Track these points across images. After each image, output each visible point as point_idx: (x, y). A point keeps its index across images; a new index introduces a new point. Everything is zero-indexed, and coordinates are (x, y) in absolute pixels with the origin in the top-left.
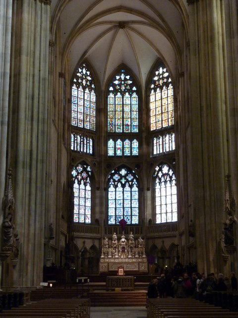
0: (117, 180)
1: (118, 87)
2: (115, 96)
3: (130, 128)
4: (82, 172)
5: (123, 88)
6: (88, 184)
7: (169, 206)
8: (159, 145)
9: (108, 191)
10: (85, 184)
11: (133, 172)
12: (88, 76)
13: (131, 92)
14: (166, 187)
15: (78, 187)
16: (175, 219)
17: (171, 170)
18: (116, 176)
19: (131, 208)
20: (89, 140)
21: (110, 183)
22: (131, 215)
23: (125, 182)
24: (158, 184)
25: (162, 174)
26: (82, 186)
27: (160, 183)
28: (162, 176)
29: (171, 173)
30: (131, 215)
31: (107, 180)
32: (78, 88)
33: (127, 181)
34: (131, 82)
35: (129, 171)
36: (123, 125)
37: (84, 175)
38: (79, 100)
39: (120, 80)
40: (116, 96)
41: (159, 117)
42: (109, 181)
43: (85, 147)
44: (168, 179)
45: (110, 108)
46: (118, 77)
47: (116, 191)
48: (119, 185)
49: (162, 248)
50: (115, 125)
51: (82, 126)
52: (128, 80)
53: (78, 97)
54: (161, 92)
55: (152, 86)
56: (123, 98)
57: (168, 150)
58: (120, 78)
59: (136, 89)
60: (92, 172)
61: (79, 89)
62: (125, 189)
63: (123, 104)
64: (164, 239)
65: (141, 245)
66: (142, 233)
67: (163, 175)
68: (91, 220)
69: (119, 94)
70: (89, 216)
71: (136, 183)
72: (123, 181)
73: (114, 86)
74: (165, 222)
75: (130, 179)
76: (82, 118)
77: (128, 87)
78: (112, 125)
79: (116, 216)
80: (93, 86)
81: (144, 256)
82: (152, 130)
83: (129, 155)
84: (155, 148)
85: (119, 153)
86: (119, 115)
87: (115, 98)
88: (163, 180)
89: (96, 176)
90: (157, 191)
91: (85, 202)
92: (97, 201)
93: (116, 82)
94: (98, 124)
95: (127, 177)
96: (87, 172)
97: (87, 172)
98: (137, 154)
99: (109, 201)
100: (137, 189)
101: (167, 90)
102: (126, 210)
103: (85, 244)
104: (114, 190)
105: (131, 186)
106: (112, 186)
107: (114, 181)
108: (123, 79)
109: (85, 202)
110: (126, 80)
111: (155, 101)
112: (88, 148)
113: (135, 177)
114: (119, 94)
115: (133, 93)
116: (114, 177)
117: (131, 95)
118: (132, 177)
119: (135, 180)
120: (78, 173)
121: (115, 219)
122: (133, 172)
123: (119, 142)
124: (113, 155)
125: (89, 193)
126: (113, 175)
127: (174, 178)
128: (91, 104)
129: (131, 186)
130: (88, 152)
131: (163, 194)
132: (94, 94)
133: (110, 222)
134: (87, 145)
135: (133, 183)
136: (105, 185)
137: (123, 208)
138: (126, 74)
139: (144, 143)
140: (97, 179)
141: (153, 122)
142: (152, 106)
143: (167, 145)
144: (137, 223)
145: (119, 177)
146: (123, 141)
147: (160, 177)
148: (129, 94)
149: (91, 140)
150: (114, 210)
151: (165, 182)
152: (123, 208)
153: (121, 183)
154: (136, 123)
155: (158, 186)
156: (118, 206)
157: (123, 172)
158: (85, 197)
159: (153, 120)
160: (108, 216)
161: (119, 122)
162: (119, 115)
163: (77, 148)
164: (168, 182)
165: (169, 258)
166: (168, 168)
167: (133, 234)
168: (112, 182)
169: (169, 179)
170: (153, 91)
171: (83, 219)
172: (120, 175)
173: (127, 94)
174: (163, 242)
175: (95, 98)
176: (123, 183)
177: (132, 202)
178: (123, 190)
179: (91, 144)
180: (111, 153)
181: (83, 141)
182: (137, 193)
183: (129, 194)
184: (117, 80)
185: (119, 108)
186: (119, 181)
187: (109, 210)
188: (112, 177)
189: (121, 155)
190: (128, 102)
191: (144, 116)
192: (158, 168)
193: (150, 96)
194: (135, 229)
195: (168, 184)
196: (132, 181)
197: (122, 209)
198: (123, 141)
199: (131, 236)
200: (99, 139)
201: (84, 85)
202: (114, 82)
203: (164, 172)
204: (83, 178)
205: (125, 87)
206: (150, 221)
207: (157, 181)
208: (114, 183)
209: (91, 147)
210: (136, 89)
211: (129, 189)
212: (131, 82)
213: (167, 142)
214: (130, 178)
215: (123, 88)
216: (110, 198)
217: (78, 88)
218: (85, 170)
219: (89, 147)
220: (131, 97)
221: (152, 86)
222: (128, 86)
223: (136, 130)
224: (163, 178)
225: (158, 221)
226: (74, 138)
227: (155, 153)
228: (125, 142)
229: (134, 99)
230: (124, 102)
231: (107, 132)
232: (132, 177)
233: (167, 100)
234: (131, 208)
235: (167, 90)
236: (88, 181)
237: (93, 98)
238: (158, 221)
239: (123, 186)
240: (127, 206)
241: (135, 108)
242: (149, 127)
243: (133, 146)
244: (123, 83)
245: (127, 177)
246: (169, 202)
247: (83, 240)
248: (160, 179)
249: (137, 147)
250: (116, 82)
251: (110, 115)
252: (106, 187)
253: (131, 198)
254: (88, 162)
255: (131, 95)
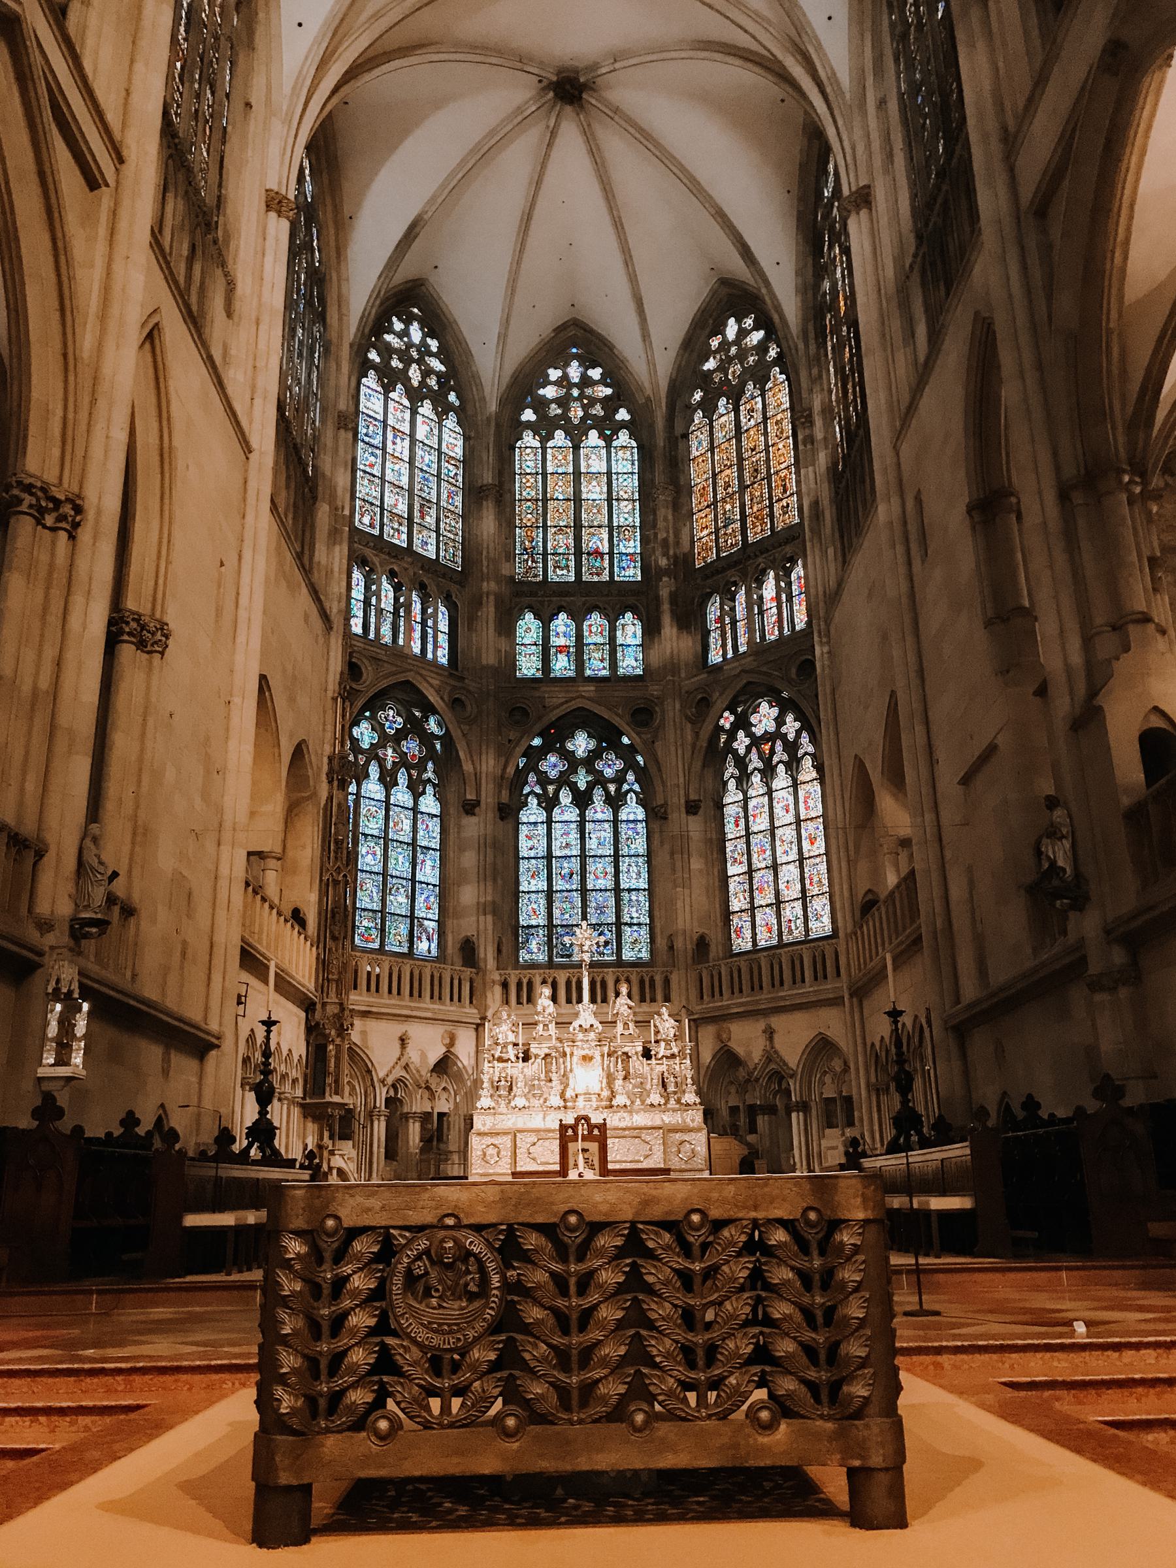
0: (553, 774)
1: (555, 410)
2: (544, 441)
3: (606, 564)
4: (400, 736)
5: (576, 413)
6: (429, 789)
7: (789, 873)
8: (734, 622)
9: (518, 823)
10: (416, 789)
11: (625, 740)
12: (431, 354)
13: (608, 428)
14: (770, 793)
15: (381, 796)
16: (822, 925)
17: (790, 718)
18: (552, 759)
19: (617, 890)
20: (436, 610)
21: (527, 790)
22: (619, 924)
23: (591, 786)
24: (732, 784)
25: (747, 741)
26: (402, 795)
27: (743, 779)
28: (748, 749)
29: (791, 726)
30: (619, 924)
31: (511, 770)
32: (387, 389)
33: (599, 780)
34: (609, 391)
35: (607, 737)
36: (578, 553)
37: (411, 746)
38: (390, 435)
39: (564, 381)
40: (550, 444)
41: (731, 508)
42: (520, 779)
43: (417, 635)
44: (780, 755)
45: (525, 488)
46: (554, 374)
47: (549, 822)
48: (565, 797)
49: (769, 1060)
50: (545, 554)
51: (401, 541)
52: (596, 383)
53: (385, 422)
54: (736, 410)
55: (698, 396)
56: (576, 448)
57: (772, 636)
58: (565, 377)
59: (627, 417)
60: (447, 740)
61: (392, 395)
62: (589, 814)
63: (577, 474)
64: (776, 1021)
65: (667, 1042)
66: (667, 999)
67: (756, 742)
68: (441, 946)
69: (559, 435)
70: (431, 926)
71: (636, 787)
72: (582, 780)
73: (540, 405)
74: (775, 942)
75: (609, 772)
76: (402, 508)
77: (598, 410)
78: (530, 552)
79: (550, 926)
80: (452, 397)
81: (690, 1097)
82: (699, 564)
83: (605, 673)
84: (714, 638)
85: (562, 665)
86: (560, 514)
87: (544, 449)
88: (755, 762)
89: (462, 754)
90: (732, 811)
91: (414, 865)
92: (469, 860)
93: (550, 392)
94: (469, 546)
95: (599, 765)
96: (426, 739)
97: (426, 739)
98: (639, 672)
99: (523, 865)
100: (640, 814)
101: (763, 395)
102: (594, 899)
103: (408, 1050)
104: (543, 816)
105: (615, 802)
106: (532, 801)
107: (543, 780)
108: (576, 380)
109: (414, 865)
110: (586, 382)
111: (712, 449)
112: (430, 639)
113: (631, 765)
114: (559, 435)
115: (615, 432)
116: (544, 766)
117: (609, 441)
118: (619, 765)
119: (631, 777)
120: (384, 739)
121: (549, 942)
122: (625, 740)
123: (562, 623)
124: (539, 675)
125: (435, 826)
126: (535, 756)
127: (806, 746)
128: (444, 464)
129: (615, 802)
130: (430, 656)
131: (760, 823)
132: (458, 429)
133: (524, 956)
134: (424, 623)
135: (625, 787)
136: (505, 794)
137: (584, 891)
138: (588, 362)
139: (667, 619)
140: (467, 767)
141: (705, 532)
142: (698, 475)
143: (771, 617)
144: (645, 955)
145: (562, 766)
146: (578, 617)
147: (742, 751)
148: (602, 435)
149: (442, 609)
150: (543, 902)
151: (768, 772)
152: (584, 891)
153: (573, 787)
154: (632, 546)
155: (732, 795)
156: (559, 884)
157: (581, 744)
158: (413, 844)
159: (702, 528)
160: (516, 926)
161: (564, 542)
162: (560, 514)
163: (378, 630)
164: (781, 768)
165: (804, 1107)
166: (775, 712)
167: (629, 996)
168: (532, 785)
169: (785, 757)
170: (698, 416)
171: (404, 938)
172: (568, 756)
173: (593, 434)
174: (770, 1033)
175: (460, 443)
176: (582, 786)
177: (623, 867)
178: (582, 815)
179: (443, 626)
180: (528, 666)
181: (408, 606)
182: (641, 827)
183: (607, 833)
184: (551, 383)
185: (560, 490)
186: (564, 780)
187: (523, 901)
188: (532, 767)
189: (571, 674)
190: (599, 465)
191: (664, 514)
192: (732, 718)
193: (686, 436)
194: (634, 979)
195: (781, 780)
196: (620, 779)
197: (577, 898)
198: (578, 617)
199: (622, 1005)
200: (477, 602)
201: (415, 383)
202: (541, 392)
203: (758, 731)
204: (403, 761)
205: (584, 407)
206: (702, 944)
207: (731, 770)
208: (545, 790)
209: (443, 640)
210: (627, 417)
211: (608, 814)
212: (609, 391)
213: (770, 605)
214: (610, 767)
215: (576, 413)
216: (524, 852)
217: (387, 389)
218: (414, 728)
219: (435, 637)
220: (608, 447)
221: (698, 396)
222: (598, 406)
223: (632, 573)
224: (754, 755)
225: (742, 943)
226: (367, 588)
227: (715, 657)
228: (586, 623)
229: (620, 453)
230: (583, 464)
231: (512, 578)
232: (619, 765)
233: (766, 434)
234: (617, 890)
235: (763, 395)
236: (429, 774)
237: (454, 444)
238: (742, 943)
239: (582, 800)
240: (602, 883)
241: (628, 485)
242: (689, 557)
243: (620, 641)
244: (575, 392)
245: (599, 765)
246: (786, 854)
247: (397, 1029)
248: (741, 763)
249: (638, 641)
250: (550, 392)
251: (526, 514)
252: (505, 796)
253: (616, 850)
254: (433, 698)
255: (609, 441)
